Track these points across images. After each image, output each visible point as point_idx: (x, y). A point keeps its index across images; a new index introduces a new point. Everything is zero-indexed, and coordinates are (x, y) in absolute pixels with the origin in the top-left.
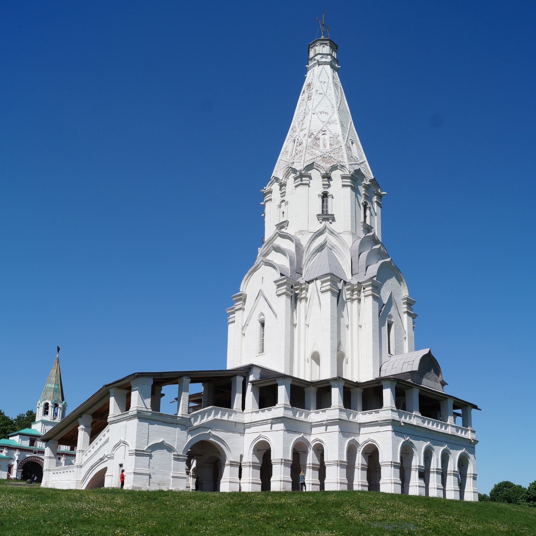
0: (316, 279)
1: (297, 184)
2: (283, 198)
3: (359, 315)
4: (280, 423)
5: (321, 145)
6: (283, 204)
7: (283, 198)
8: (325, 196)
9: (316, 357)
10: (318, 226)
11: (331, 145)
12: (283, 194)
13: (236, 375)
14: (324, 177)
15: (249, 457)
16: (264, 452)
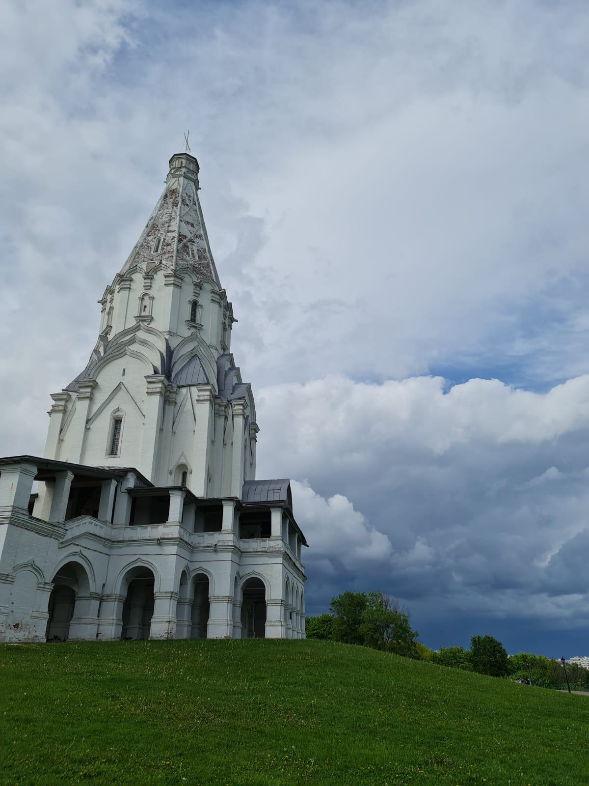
0: (193, 385)
1: (168, 282)
2: (147, 292)
3: (225, 432)
4: (174, 545)
5: (191, 254)
6: (146, 298)
7: (147, 292)
8: (195, 305)
9: (184, 472)
10: (186, 332)
11: (199, 257)
12: (148, 287)
13: (111, 479)
14: (196, 285)
15: (117, 587)
16: (141, 583)
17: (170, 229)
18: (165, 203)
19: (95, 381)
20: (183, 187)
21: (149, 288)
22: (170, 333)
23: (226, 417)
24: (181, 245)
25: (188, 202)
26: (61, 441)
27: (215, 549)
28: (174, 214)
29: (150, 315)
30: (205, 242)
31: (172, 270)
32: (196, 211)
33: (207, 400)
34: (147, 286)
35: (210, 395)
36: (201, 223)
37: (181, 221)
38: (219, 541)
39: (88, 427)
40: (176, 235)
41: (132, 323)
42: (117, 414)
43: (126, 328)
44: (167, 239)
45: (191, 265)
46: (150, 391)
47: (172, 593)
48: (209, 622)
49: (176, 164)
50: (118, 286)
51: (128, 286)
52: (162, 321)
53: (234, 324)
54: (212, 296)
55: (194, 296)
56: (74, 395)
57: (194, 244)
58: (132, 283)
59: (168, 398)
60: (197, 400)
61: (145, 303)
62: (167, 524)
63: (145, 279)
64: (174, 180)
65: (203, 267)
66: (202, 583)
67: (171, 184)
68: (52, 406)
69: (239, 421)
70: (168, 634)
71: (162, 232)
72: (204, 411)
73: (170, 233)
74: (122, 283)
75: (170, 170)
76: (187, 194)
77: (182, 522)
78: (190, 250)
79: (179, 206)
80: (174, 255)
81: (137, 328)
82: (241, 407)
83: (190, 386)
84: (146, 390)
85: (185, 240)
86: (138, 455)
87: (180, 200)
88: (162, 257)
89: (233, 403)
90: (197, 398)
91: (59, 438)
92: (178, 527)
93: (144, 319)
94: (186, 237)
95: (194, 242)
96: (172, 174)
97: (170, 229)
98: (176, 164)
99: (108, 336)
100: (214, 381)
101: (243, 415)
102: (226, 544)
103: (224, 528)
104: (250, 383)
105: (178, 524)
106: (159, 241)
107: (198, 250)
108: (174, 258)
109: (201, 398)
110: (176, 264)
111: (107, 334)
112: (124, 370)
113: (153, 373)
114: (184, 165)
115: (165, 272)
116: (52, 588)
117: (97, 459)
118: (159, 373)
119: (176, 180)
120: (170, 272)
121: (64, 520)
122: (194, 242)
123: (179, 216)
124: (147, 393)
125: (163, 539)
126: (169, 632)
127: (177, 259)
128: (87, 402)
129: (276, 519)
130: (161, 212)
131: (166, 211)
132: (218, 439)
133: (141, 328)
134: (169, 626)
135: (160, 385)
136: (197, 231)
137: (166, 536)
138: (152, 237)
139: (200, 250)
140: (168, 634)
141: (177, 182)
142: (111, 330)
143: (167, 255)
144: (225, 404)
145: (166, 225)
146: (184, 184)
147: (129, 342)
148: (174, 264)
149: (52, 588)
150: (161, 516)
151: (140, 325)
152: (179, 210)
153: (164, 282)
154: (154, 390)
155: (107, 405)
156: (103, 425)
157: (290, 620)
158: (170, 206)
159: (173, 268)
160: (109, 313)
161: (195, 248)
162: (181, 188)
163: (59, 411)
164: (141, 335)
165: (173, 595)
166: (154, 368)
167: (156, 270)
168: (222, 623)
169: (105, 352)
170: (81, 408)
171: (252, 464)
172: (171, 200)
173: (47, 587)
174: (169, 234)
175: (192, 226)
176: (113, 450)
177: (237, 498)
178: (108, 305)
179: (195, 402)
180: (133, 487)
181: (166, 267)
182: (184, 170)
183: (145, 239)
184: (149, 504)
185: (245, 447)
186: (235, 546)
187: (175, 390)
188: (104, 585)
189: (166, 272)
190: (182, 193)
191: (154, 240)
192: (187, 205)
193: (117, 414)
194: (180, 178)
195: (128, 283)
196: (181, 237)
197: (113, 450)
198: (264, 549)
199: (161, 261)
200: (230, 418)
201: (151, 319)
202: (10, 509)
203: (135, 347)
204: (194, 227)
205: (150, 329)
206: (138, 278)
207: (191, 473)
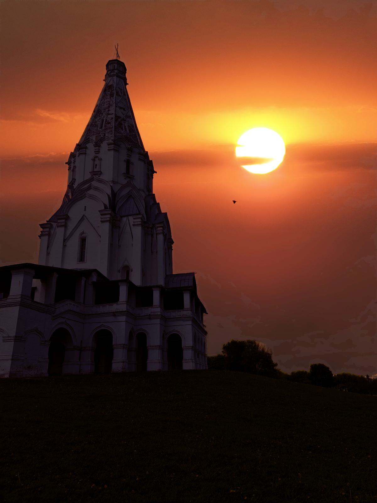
0: (130, 215)
1: (110, 148)
2: (97, 155)
6: (97, 159)
7: (97, 155)
8: (128, 163)
9: (127, 270)
10: (124, 181)
11: (129, 130)
12: (98, 152)
16: (104, 338)
17: (110, 112)
18: (105, 95)
19: (67, 215)
20: (116, 83)
21: (98, 152)
22: (113, 182)
23: (152, 236)
24: (117, 123)
25: (120, 94)
26: (48, 254)
27: (150, 317)
28: (111, 102)
29: (100, 170)
30: (133, 120)
31: (112, 140)
32: (126, 99)
33: (139, 225)
34: (97, 151)
35: (141, 221)
36: (129, 108)
37: (117, 107)
38: (151, 312)
39: (65, 244)
40: (113, 116)
41: (88, 176)
42: (83, 235)
43: (85, 180)
44: (108, 119)
45: (124, 136)
46: (103, 220)
47: (124, 344)
48: (148, 362)
49: (111, 67)
50: (78, 152)
51: (84, 152)
52: (108, 174)
53: (155, 175)
54: (139, 157)
55: (128, 156)
56: (54, 225)
57: (126, 122)
58: (87, 150)
59: (115, 225)
60: (133, 225)
61: (96, 163)
62: (119, 303)
63: (95, 147)
64: (110, 78)
65: (132, 137)
66: (142, 338)
67: (109, 81)
68: (41, 232)
69: (161, 238)
70: (123, 369)
71: (104, 114)
72: (138, 232)
73: (109, 116)
74: (80, 150)
75: (107, 72)
76: (119, 88)
77: (128, 302)
78: (123, 126)
79: (114, 96)
80: (113, 130)
81: (92, 179)
82: (161, 228)
83: (128, 216)
84: (100, 219)
85: (119, 120)
86: (98, 261)
87: (115, 92)
88: (105, 132)
89: (157, 226)
90: (133, 223)
91: (47, 252)
92: (125, 305)
93: (96, 173)
94: (120, 117)
95: (125, 121)
96: (108, 74)
97: (109, 113)
98: (111, 67)
99: (73, 185)
100: (143, 212)
101: (163, 234)
102: (156, 314)
103: (154, 304)
104: (166, 213)
105: (125, 302)
106: (103, 120)
107: (128, 126)
108: (113, 132)
109: (136, 223)
110: (115, 136)
111: (73, 184)
112: (85, 207)
113: (104, 208)
114: (116, 68)
115: (108, 142)
116: (50, 344)
117: (72, 264)
118: (108, 209)
119: (111, 79)
120: (111, 141)
121: (54, 303)
122: (125, 121)
123: (115, 103)
124: (101, 221)
125: (117, 312)
126: (124, 368)
127: (115, 133)
128: (63, 228)
129: (187, 298)
130: (103, 101)
131: (106, 100)
132: (148, 249)
133: (95, 179)
134: (123, 364)
135: (109, 216)
136: (127, 113)
137: (118, 311)
138: (98, 118)
139: (130, 125)
140: (123, 369)
141: (112, 80)
142: (75, 182)
143: (109, 130)
144: (151, 226)
145: (107, 110)
146: (117, 81)
147: (87, 189)
148: (113, 136)
149: (50, 344)
150: (115, 299)
151: (93, 177)
152: (114, 99)
153: (108, 149)
154: (105, 219)
155: (75, 230)
156: (74, 243)
157: (198, 359)
158: (108, 97)
159: (113, 138)
160: (73, 171)
161: (126, 125)
162: (115, 84)
163: (46, 235)
164: (95, 184)
165: (125, 346)
166: (104, 205)
167: (102, 140)
168: (155, 361)
169: (72, 196)
170: (59, 233)
171: (171, 264)
172: (109, 92)
173: (47, 343)
174: (109, 116)
175: (123, 110)
176: (82, 259)
177: (162, 286)
178: (72, 165)
179: (132, 226)
180: (96, 281)
181: (108, 138)
182: (116, 71)
183: (93, 120)
184: (106, 290)
185: (165, 254)
186: (161, 315)
187: (119, 219)
188: (82, 341)
189: (108, 142)
190: (116, 87)
191: (99, 120)
192: (120, 96)
193: (82, 236)
194: (114, 77)
195: (84, 150)
196: (117, 118)
197: (82, 259)
198: (180, 316)
199: (105, 134)
200: (155, 236)
201: (100, 173)
202: (20, 296)
203: (91, 192)
204: (125, 111)
205: (100, 180)
206: (90, 146)
207: (132, 271)
